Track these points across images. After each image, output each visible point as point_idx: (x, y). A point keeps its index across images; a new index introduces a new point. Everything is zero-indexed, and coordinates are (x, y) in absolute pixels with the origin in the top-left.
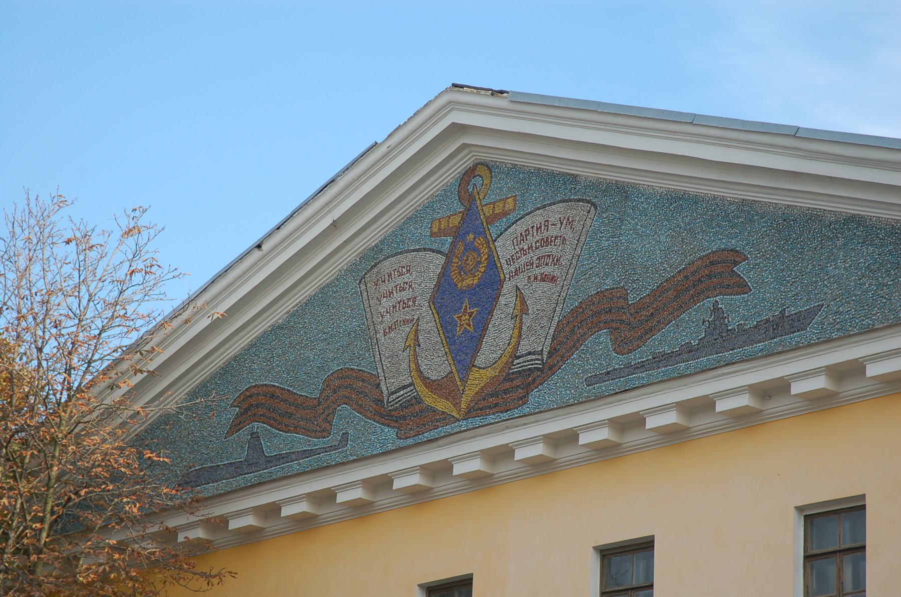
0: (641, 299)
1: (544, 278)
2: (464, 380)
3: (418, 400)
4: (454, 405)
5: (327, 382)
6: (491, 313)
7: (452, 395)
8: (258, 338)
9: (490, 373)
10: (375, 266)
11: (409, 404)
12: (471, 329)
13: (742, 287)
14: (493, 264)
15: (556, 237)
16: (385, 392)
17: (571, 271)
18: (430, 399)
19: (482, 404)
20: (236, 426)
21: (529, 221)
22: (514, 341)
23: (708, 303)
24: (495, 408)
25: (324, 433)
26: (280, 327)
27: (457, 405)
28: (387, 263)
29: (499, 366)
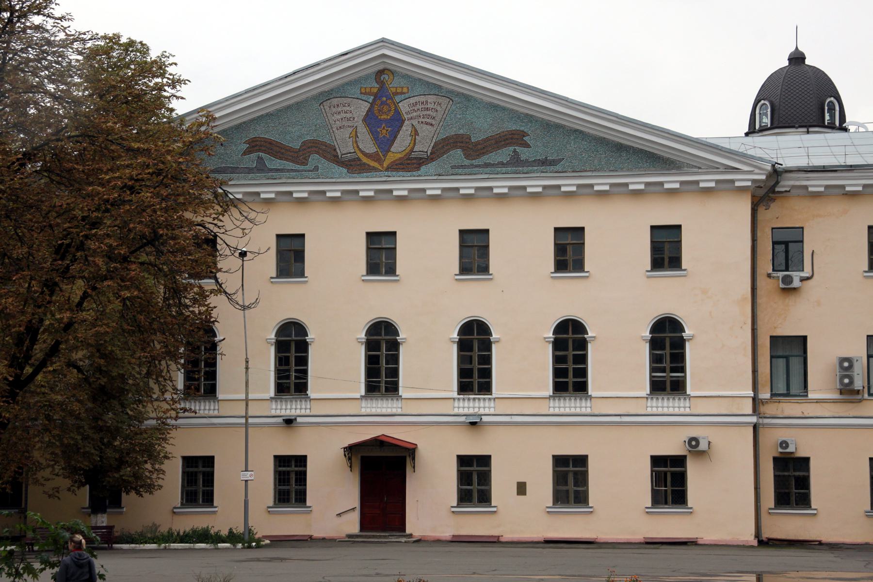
1: (427, 124)
2: (385, 156)
3: (359, 159)
4: (380, 165)
6: (398, 131)
8: (258, 117)
9: (399, 156)
10: (329, 99)
11: (354, 160)
13: (528, 146)
14: (398, 112)
15: (432, 109)
16: (339, 154)
17: (441, 123)
18: (365, 160)
19: (395, 167)
20: (246, 153)
21: (416, 99)
22: (412, 145)
23: (512, 148)
24: (403, 170)
27: (381, 165)
28: (336, 99)
29: (404, 153)
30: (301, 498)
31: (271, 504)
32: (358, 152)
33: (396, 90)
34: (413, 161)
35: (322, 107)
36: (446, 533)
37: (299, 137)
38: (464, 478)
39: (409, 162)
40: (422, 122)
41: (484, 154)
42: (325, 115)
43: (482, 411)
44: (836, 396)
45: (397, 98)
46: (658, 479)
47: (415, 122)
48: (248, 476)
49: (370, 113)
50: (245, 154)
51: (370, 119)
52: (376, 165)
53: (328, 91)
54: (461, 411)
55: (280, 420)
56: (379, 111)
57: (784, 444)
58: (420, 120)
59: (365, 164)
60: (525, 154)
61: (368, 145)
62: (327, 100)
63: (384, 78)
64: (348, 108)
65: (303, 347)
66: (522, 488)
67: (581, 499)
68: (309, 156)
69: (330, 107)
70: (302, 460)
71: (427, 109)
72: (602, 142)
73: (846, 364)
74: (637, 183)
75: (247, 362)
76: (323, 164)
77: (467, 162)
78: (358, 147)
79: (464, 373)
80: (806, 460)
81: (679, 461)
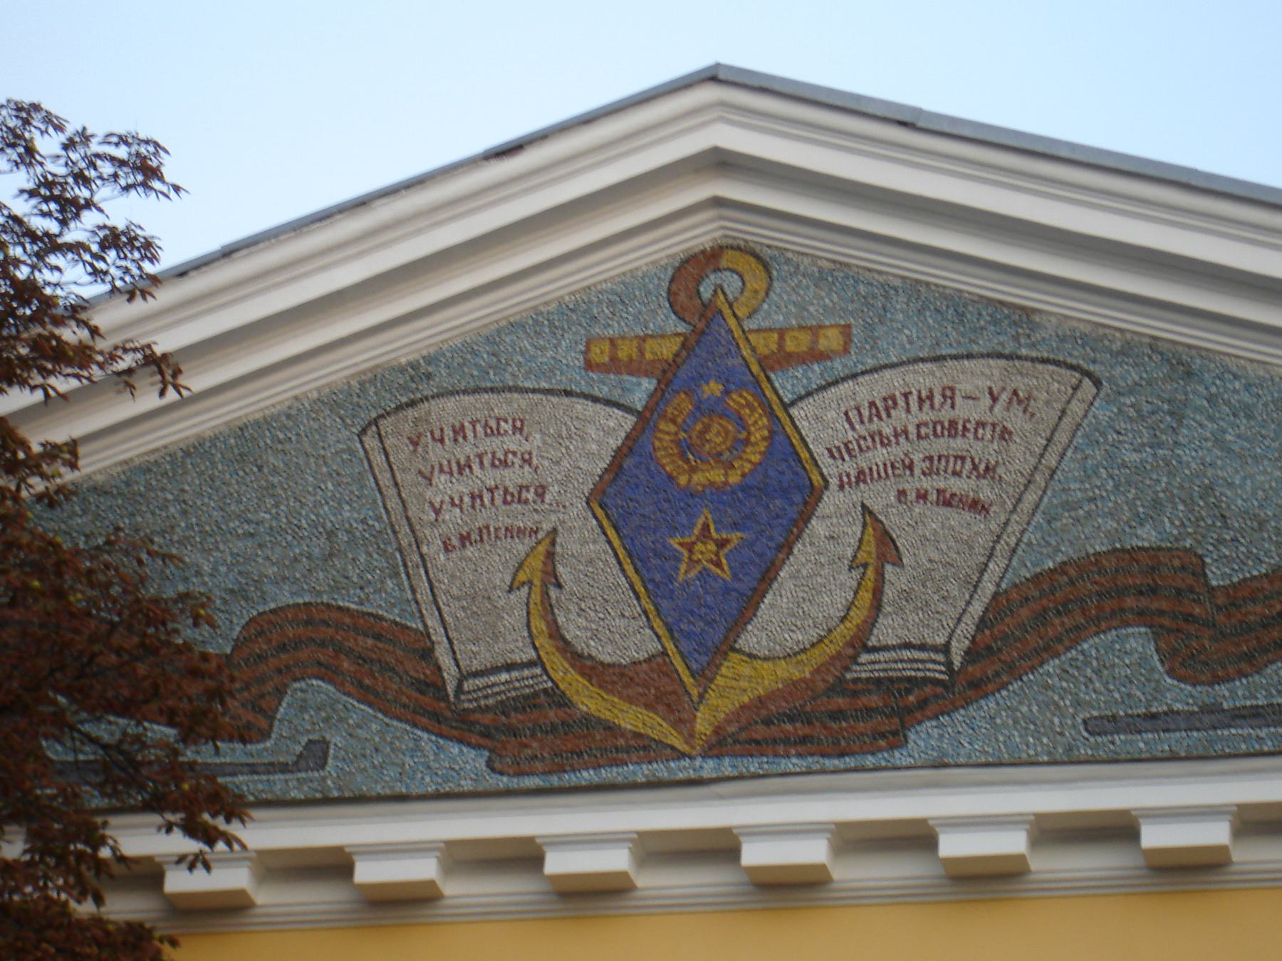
0: (1245, 580)
1: (946, 500)
2: (704, 676)
3: (558, 698)
6: (786, 548)
10: (412, 404)
11: (528, 702)
17: (1030, 498)
19: (760, 732)
21: (892, 381)
22: (858, 616)
27: (682, 723)
28: (450, 404)
33: (782, 338)
34: (864, 700)
35: (371, 442)
39: (841, 701)
40: (922, 496)
42: (385, 479)
45: (786, 383)
47: (880, 497)
49: (628, 463)
53: (414, 365)
56: (684, 449)
58: (911, 485)
59: (588, 721)
62: (400, 408)
63: (719, 288)
64: (512, 442)
68: (280, 692)
71: (952, 428)
78: (556, 633)
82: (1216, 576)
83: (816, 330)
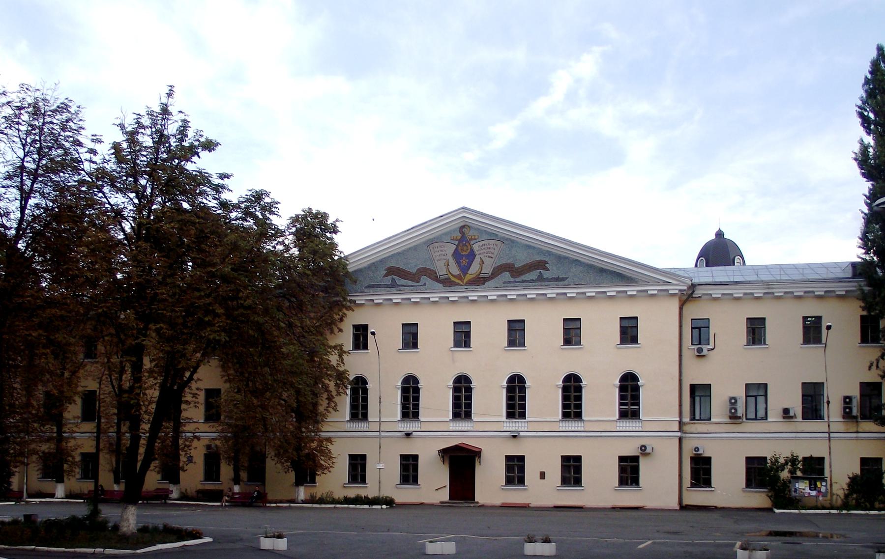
3: (450, 279)
5: (419, 269)
7: (461, 279)
9: (473, 276)
11: (446, 279)
12: (466, 264)
14: (472, 250)
18: (453, 279)
20: (386, 276)
25: (418, 282)
26: (400, 253)
27: (463, 282)
29: (476, 275)
30: (415, 481)
31: (398, 482)
32: (449, 274)
36: (498, 502)
37: (415, 266)
38: (509, 469)
39: (478, 280)
41: (522, 274)
43: (520, 429)
44: (728, 420)
45: (472, 242)
46: (622, 470)
47: (482, 256)
48: (381, 466)
50: (384, 276)
51: (456, 255)
52: (460, 282)
54: (508, 429)
55: (403, 434)
57: (697, 449)
59: (453, 281)
60: (546, 274)
61: (455, 270)
65: (417, 390)
66: (543, 475)
67: (578, 482)
69: (433, 248)
70: (416, 458)
71: (489, 248)
72: (591, 267)
73: (733, 401)
74: (611, 291)
75: (380, 398)
76: (429, 282)
77: (512, 280)
79: (510, 406)
80: (710, 458)
81: (635, 459)
82: (516, 266)
83: (475, 236)
